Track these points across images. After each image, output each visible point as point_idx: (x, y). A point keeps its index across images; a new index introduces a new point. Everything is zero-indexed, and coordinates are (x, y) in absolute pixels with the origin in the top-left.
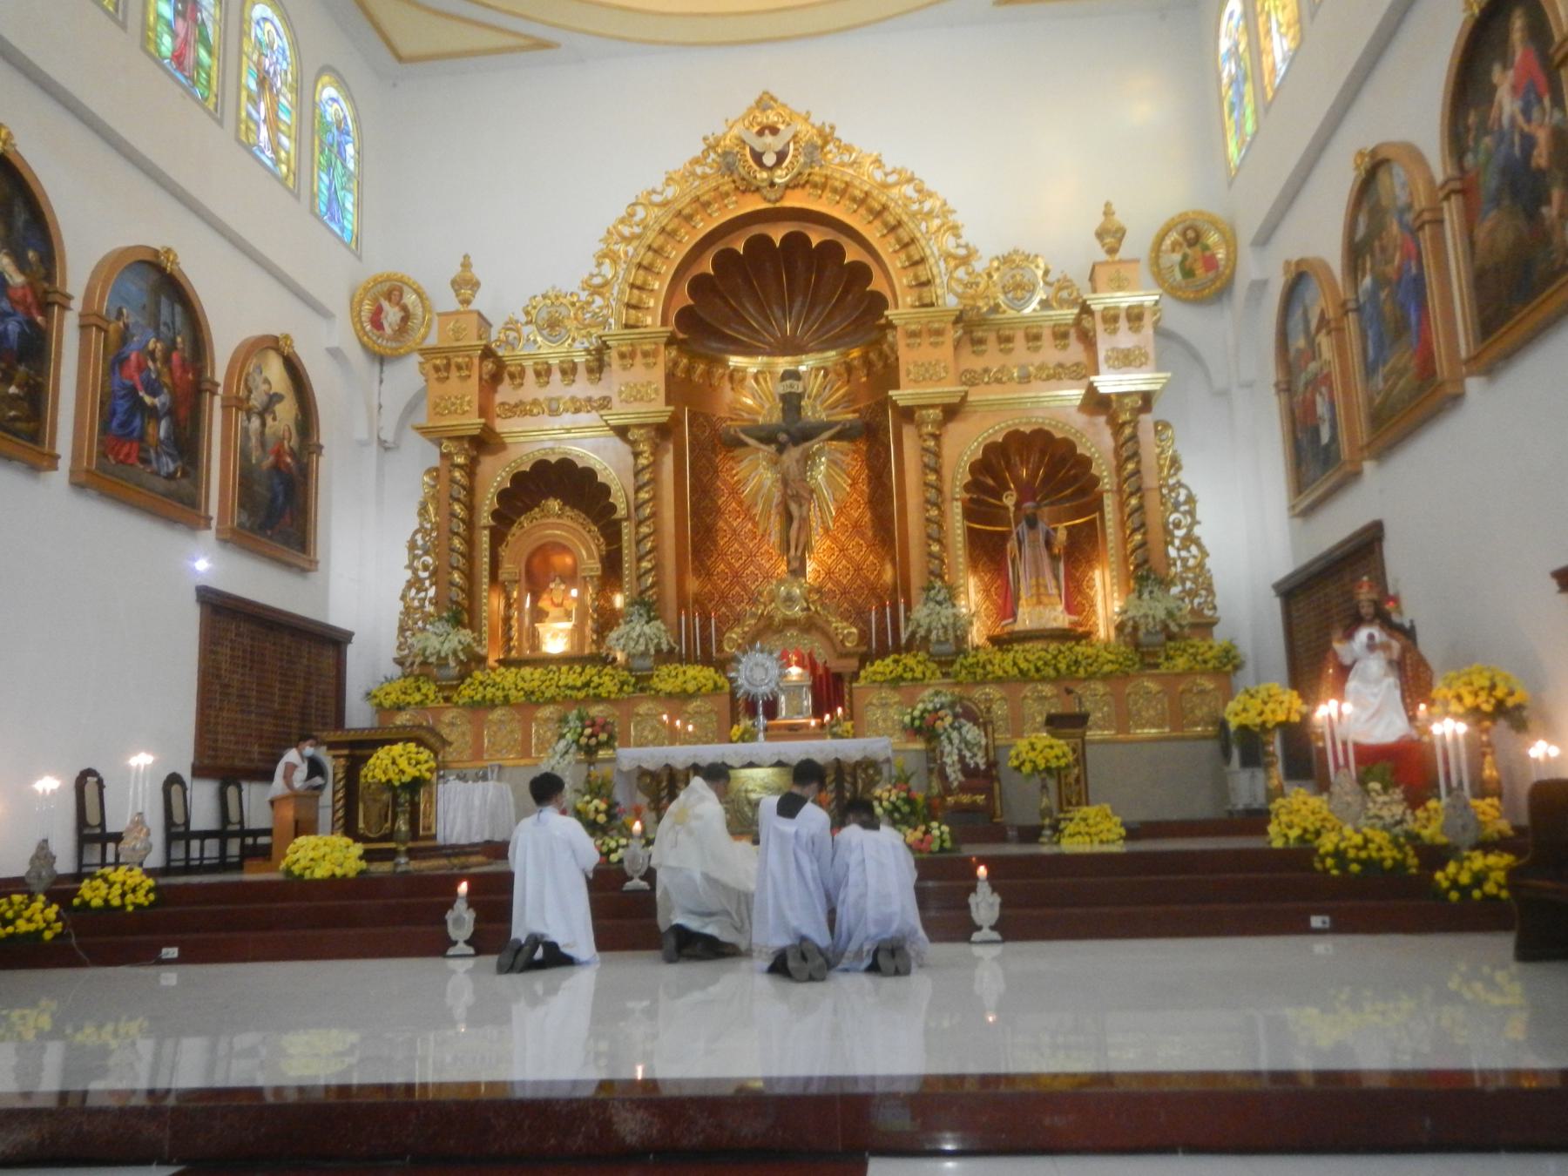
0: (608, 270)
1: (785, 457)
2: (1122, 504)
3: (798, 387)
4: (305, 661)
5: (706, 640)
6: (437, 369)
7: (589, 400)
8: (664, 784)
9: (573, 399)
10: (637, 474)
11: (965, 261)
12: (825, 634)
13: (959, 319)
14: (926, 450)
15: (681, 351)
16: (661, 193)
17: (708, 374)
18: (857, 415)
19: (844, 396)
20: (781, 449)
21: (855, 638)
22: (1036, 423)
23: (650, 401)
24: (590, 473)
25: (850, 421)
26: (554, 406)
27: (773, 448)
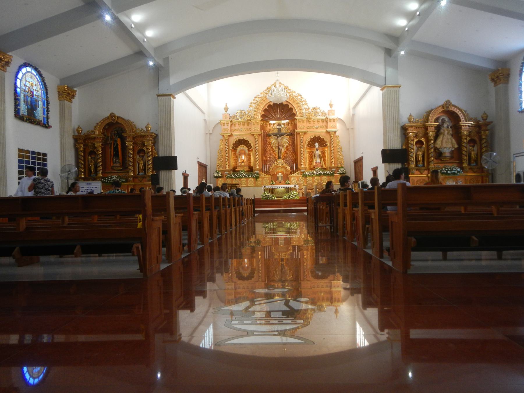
0: (252, 108)
1: (278, 139)
2: (331, 149)
3: (280, 127)
5: (266, 168)
6: (223, 124)
7: (247, 129)
11: (308, 109)
12: (286, 168)
13: (307, 119)
16: (260, 96)
17: (266, 124)
20: (278, 137)
21: (290, 169)
24: (247, 141)
27: (276, 137)
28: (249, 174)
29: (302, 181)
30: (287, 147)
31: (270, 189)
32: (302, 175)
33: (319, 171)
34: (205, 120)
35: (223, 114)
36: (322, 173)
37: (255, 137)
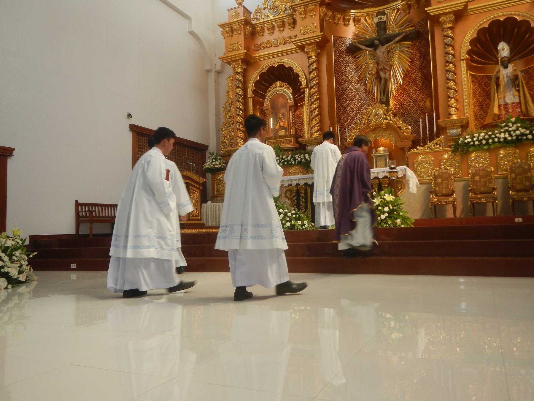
1: (378, 51)
3: (384, 18)
4: (187, 157)
6: (227, 32)
8: (294, 194)
9: (284, 38)
10: (309, 66)
14: (447, 36)
15: (327, 8)
18: (413, 28)
19: (406, 20)
20: (375, 47)
22: (508, 15)
23: (314, 32)
24: (291, 69)
25: (410, 30)
26: (275, 43)
27: (371, 49)
28: (290, 156)
29: (451, 166)
30: (406, 75)
31: (298, 191)
32: (450, 146)
33: (514, 128)
34: (192, 33)
35: (229, 10)
36: (526, 135)
37: (307, 53)
